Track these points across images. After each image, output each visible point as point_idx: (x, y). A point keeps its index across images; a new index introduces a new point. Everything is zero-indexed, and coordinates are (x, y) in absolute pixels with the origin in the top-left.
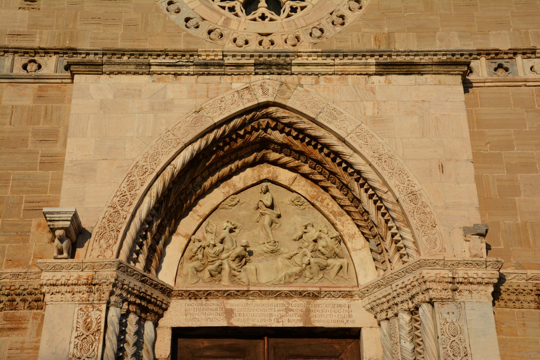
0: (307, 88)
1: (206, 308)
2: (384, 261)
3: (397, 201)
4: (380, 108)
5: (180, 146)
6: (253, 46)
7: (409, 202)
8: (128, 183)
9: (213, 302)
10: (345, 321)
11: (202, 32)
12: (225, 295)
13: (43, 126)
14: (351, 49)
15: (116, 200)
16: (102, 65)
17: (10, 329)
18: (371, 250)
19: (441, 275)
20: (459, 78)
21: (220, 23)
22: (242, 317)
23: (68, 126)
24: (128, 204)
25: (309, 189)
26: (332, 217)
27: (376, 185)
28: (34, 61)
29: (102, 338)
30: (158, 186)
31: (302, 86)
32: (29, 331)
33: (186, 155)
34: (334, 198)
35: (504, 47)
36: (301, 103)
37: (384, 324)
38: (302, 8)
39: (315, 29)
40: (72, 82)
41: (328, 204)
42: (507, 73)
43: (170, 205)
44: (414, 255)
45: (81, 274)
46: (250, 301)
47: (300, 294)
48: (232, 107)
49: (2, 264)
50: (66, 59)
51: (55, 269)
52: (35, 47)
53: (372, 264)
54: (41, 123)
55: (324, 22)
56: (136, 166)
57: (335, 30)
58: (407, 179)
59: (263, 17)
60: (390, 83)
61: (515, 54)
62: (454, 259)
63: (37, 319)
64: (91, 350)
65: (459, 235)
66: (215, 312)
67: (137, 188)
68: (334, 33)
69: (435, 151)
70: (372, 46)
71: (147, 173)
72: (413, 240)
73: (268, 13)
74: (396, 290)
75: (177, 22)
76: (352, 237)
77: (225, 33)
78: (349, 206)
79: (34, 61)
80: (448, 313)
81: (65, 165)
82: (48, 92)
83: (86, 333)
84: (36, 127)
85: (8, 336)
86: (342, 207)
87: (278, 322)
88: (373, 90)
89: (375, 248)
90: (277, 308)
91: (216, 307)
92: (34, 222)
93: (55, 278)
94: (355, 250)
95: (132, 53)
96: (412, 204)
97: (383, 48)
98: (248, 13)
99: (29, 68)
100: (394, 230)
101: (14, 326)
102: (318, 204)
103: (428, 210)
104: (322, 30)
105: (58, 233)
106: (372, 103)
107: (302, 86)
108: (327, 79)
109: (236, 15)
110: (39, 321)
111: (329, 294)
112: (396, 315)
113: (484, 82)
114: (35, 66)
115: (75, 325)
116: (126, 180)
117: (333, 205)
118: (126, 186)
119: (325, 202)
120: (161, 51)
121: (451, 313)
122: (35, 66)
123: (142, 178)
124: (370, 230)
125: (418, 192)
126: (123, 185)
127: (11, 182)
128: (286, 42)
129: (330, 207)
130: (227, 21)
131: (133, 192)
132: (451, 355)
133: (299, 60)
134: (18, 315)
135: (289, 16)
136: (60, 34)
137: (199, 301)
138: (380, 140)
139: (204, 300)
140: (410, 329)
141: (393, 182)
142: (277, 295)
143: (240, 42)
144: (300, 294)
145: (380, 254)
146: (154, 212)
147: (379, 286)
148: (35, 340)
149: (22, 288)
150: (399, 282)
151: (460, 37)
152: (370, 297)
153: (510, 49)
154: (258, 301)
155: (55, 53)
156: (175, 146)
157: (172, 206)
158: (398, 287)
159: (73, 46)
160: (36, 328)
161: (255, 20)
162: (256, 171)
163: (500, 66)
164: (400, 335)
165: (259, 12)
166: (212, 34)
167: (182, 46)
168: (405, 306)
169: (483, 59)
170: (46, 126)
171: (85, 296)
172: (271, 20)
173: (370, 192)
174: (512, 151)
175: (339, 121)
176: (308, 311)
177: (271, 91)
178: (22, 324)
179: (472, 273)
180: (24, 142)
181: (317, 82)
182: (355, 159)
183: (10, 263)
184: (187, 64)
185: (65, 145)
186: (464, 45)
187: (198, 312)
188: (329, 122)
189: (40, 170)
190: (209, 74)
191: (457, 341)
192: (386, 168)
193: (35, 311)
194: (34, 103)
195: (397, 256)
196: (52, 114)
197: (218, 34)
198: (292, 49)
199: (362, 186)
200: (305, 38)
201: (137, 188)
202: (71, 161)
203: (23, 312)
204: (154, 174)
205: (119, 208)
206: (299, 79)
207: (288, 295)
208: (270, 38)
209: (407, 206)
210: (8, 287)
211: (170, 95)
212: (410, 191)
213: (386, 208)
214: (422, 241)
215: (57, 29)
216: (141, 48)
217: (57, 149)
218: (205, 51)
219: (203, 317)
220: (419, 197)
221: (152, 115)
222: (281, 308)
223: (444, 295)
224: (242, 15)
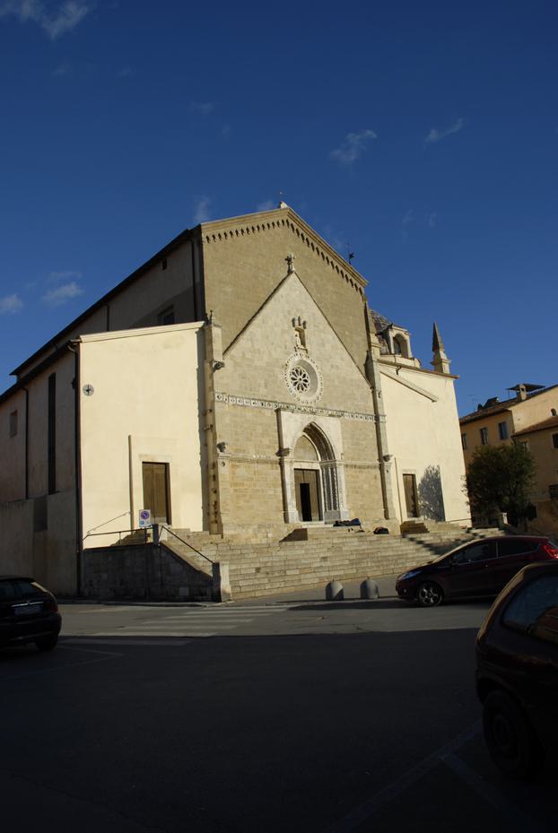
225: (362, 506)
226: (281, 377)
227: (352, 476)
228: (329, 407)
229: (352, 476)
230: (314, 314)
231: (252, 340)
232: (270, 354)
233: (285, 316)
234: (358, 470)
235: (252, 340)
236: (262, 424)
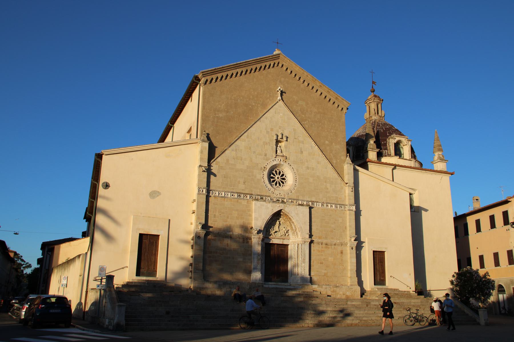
11: (270, 192)
13: (248, 209)
47: (282, 239)
111: (286, 239)
142: (279, 239)
143: (276, 194)
144: (282, 239)
167: (268, 195)
176: (283, 242)
207: (281, 239)
211: (268, 206)
225: (325, 275)
226: (259, 176)
228: (301, 198)
231: (236, 150)
233: (268, 132)
235: (236, 150)
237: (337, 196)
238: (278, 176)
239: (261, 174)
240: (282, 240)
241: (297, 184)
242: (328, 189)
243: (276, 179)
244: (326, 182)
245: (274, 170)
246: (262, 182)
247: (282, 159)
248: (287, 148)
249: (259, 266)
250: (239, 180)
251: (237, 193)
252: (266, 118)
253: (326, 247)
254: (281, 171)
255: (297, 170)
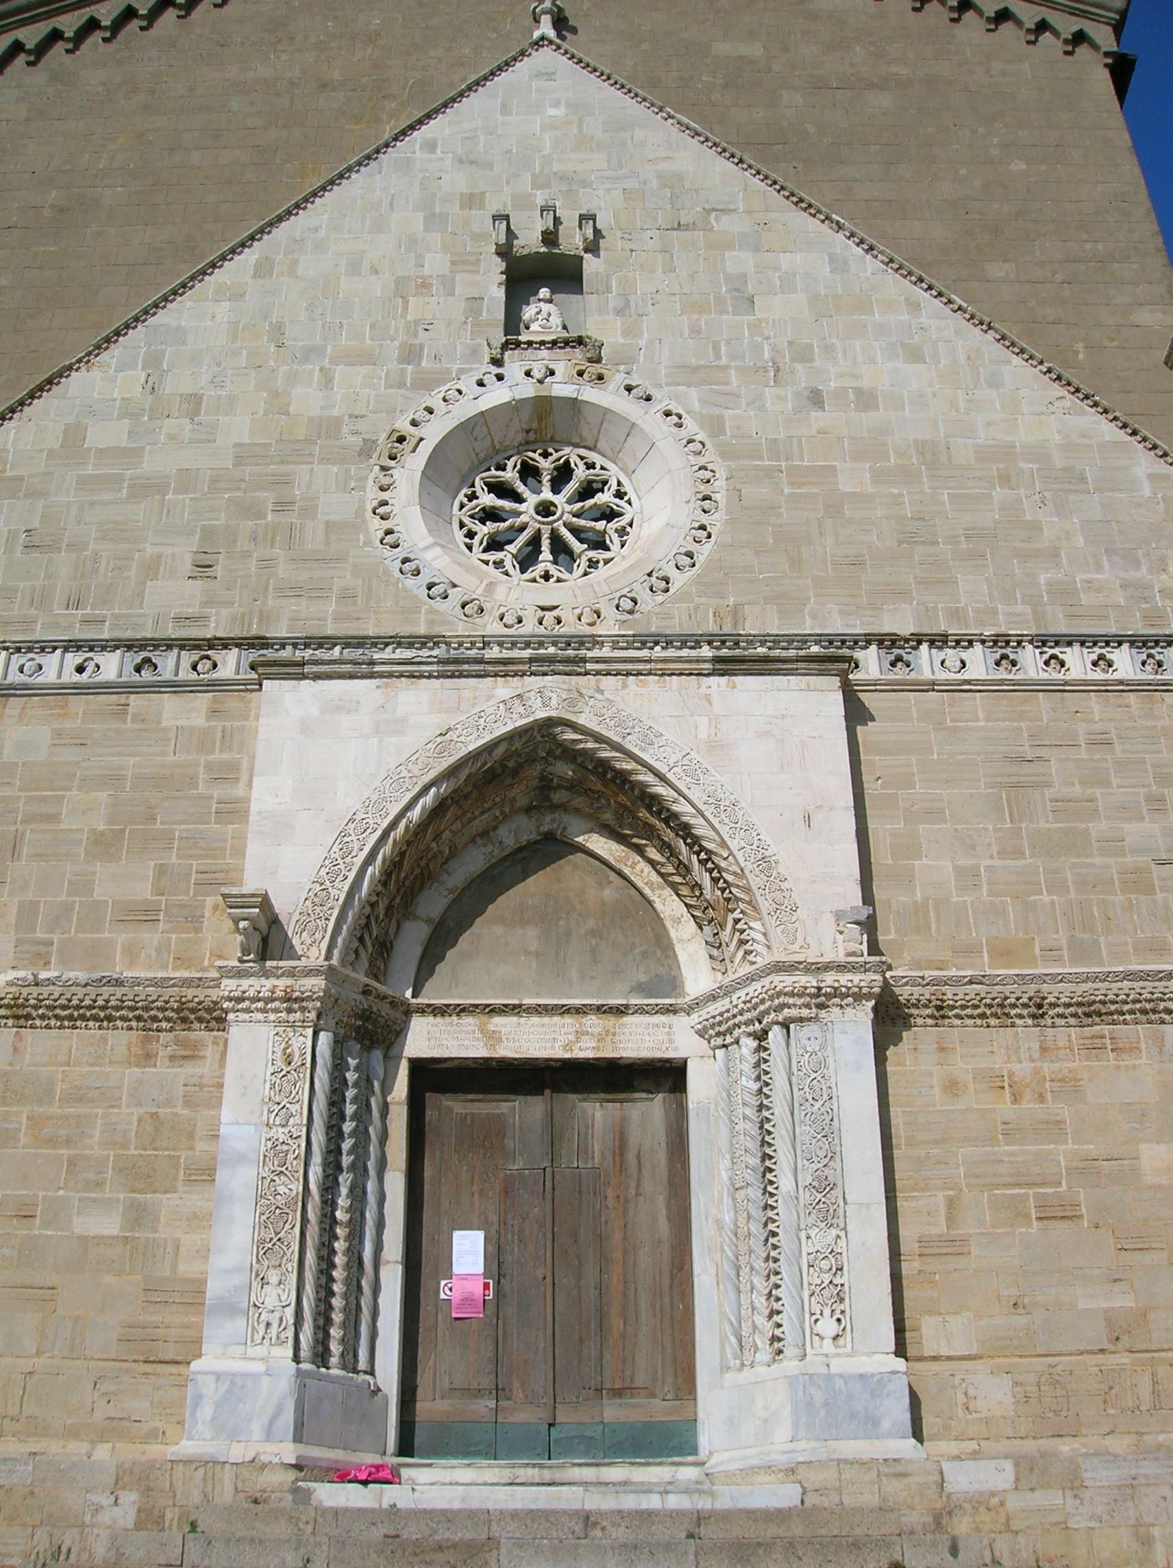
0: (609, 696)
1: (458, 1029)
2: (723, 960)
3: (742, 871)
4: (718, 726)
5: (417, 789)
6: (529, 627)
7: (758, 873)
8: (341, 846)
9: (469, 1021)
10: (664, 1049)
12: (487, 1010)
13: (218, 756)
14: (678, 631)
15: (324, 871)
16: (304, 664)
17: (184, 1057)
18: (707, 943)
19: (801, 984)
20: (836, 681)
21: (480, 591)
22: (511, 1044)
23: (254, 756)
24: (341, 878)
25: (613, 848)
26: (647, 891)
27: (710, 846)
28: (208, 657)
29: (308, 1076)
30: (387, 849)
31: (601, 692)
32: (209, 1061)
33: (429, 800)
34: (652, 863)
35: (906, 630)
36: (601, 719)
37: (720, 1053)
38: (607, 562)
39: (623, 599)
40: (260, 689)
41: (642, 871)
42: (908, 669)
43: (403, 875)
44: (765, 953)
45: (276, 982)
46: (523, 1019)
47: (600, 1010)
48: (495, 726)
49: (168, 964)
50: (253, 655)
51: (239, 974)
52: (209, 636)
53: (705, 963)
54: (217, 751)
55: (637, 587)
56: (352, 820)
57: (654, 601)
58: (756, 838)
59: (547, 577)
60: (734, 687)
61: (919, 642)
62: (819, 960)
63: (218, 1044)
64: (294, 1093)
65: (828, 925)
66: (471, 1036)
67: (354, 854)
68: (653, 604)
69: (800, 795)
70: (712, 628)
71: (369, 831)
72: (763, 930)
73: (553, 570)
74: (736, 1006)
75: (414, 589)
76: (678, 921)
77: (486, 606)
78: (673, 874)
79: (208, 657)
80: (809, 1039)
81: (251, 819)
82: (226, 705)
83: (286, 1069)
84: (210, 758)
85: (181, 1066)
86: (661, 875)
87: (565, 1050)
88: (708, 699)
89: (711, 939)
90: (563, 1031)
91: (473, 1028)
92: (210, 901)
93: (240, 989)
94: (680, 941)
95: (350, 642)
96: (762, 876)
97: (727, 629)
98: (523, 571)
99: (199, 667)
100: (737, 915)
101: (188, 1053)
102: (627, 871)
103: (785, 885)
104: (635, 601)
105: (242, 924)
106: (707, 718)
107: (601, 692)
108: (641, 681)
109: (507, 574)
110: (221, 1047)
112: (737, 1042)
113: (875, 685)
114: (208, 664)
115: (270, 1057)
116: (338, 842)
117: (649, 872)
118: (337, 850)
119: (638, 868)
120: (391, 637)
121: (812, 1039)
122: (208, 664)
123: (361, 837)
124: (703, 912)
125: (773, 858)
126: (336, 849)
127: (176, 842)
128: (580, 620)
129: (645, 874)
130: (491, 586)
131: (348, 860)
132: (810, 1099)
133: (596, 653)
134: (192, 1038)
135: (586, 574)
136: (243, 615)
137: (447, 1019)
138: (718, 777)
139: (454, 1018)
140: (755, 1061)
141: (736, 842)
144: (600, 1010)
145: (718, 948)
146: (380, 888)
147: (713, 997)
148: (217, 1073)
149: (196, 1000)
150: (742, 993)
151: (842, 612)
152: (701, 1013)
153: (912, 634)
154: (535, 1020)
155: (237, 645)
156: (410, 787)
157: (407, 877)
158: (740, 1000)
159: (261, 633)
160: (218, 1057)
161: (534, 580)
162: (533, 819)
163: (899, 659)
164: (741, 1070)
165: (540, 568)
166: (467, 607)
167: (422, 630)
168: (751, 1029)
169: (874, 647)
170: (224, 756)
171: (284, 1015)
172: (559, 580)
173: (703, 856)
174: (913, 791)
175: (656, 746)
177: (554, 702)
178: (199, 1050)
179: (844, 979)
180: (193, 781)
181: (625, 686)
182: (682, 807)
183: (179, 962)
184: (429, 660)
185: (250, 784)
186: (847, 625)
187: (446, 1036)
188: (642, 749)
189: (216, 823)
190: (461, 676)
191: (819, 1078)
192: (727, 821)
193: (215, 1033)
194: (207, 721)
195: (740, 953)
196: (232, 737)
197: (476, 608)
198: (589, 630)
199: (691, 846)
200: (608, 611)
201: (354, 854)
202: (259, 813)
203: (199, 1034)
204: (379, 832)
205: (328, 883)
206: (598, 681)
208: (555, 613)
209: (755, 882)
210: (178, 999)
212: (760, 857)
213: (725, 881)
214: (776, 933)
215: (240, 606)
216: (362, 633)
217: (240, 791)
218: (457, 636)
219: (455, 1043)
220: (774, 865)
221: (376, 740)
222: (570, 1030)
223: (805, 1012)
224: (515, 573)
227: (997, 1083)
229: (997, 1083)
230: (673, 184)
231: (153, 361)
232: (278, 403)
233: (434, 220)
234: (1067, 1035)
235: (153, 361)
236: (113, 780)
237: (1143, 573)
238: (547, 494)
239: (363, 489)
240: (592, 1020)
241: (716, 521)
242: (1036, 527)
243: (524, 518)
244: (1005, 480)
245: (510, 464)
246: (368, 543)
247: (559, 368)
248: (609, 291)
249: (273, 1277)
250: (150, 550)
251: (130, 645)
252: (431, 146)
253: (1093, 1048)
254: (573, 459)
255: (715, 426)
